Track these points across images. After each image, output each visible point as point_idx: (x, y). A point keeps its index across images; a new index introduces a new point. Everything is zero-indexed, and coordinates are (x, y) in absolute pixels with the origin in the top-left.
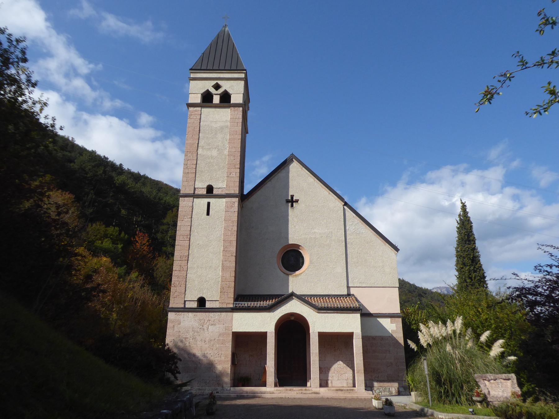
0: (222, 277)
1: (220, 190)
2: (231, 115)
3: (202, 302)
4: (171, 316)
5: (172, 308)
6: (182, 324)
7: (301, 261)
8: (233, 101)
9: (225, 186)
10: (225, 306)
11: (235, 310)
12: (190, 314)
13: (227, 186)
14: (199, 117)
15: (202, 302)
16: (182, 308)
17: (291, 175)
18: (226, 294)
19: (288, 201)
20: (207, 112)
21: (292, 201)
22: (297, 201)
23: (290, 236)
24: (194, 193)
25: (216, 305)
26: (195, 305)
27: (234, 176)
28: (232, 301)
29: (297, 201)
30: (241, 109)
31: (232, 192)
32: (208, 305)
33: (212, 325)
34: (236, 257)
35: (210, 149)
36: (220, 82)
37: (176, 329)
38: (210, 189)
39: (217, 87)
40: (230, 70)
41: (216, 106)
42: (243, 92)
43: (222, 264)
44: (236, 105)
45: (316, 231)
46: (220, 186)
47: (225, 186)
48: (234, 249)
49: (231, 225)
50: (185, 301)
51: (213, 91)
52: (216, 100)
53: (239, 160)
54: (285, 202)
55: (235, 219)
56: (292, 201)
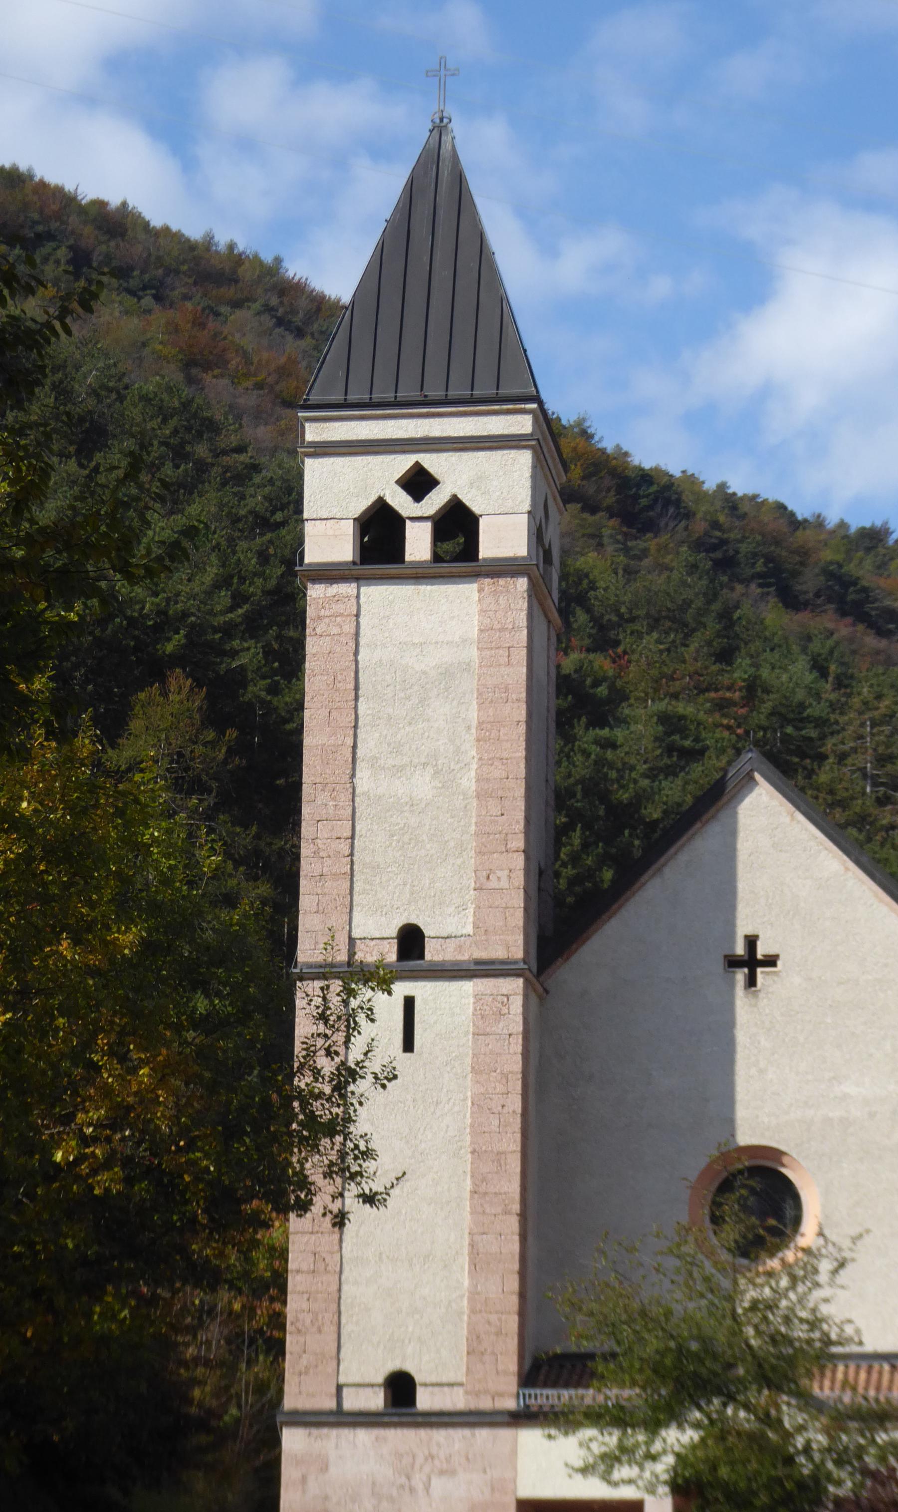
0: (473, 1294)
1: (451, 944)
2: (482, 611)
3: (401, 1388)
4: (293, 1440)
5: (295, 1413)
6: (333, 1470)
7: (789, 1213)
8: (488, 548)
9: (469, 929)
10: (485, 1404)
11: (522, 1418)
12: (363, 1436)
13: (476, 927)
14: (349, 628)
15: (401, 1388)
16: (330, 1413)
17: (744, 846)
18: (487, 1358)
19: (733, 962)
20: (380, 599)
21: (752, 962)
22: (771, 961)
23: (742, 1113)
24: (349, 964)
25: (456, 1400)
26: (376, 1400)
27: (504, 883)
28: (511, 1383)
29: (771, 961)
30: (522, 583)
31: (498, 953)
32: (424, 1400)
33: (442, 1473)
34: (523, 1216)
35: (402, 768)
36: (432, 462)
37: (313, 1487)
38: (411, 940)
39: (418, 483)
40: (471, 403)
41: (419, 575)
42: (526, 506)
43: (472, 1245)
44: (503, 569)
45: (849, 1088)
46: (451, 930)
47: (469, 929)
48: (513, 1187)
49: (500, 1088)
50: (339, 1388)
51: (401, 502)
52: (418, 543)
53: (520, 816)
54: (719, 965)
55: (515, 1064)
56: (752, 962)
